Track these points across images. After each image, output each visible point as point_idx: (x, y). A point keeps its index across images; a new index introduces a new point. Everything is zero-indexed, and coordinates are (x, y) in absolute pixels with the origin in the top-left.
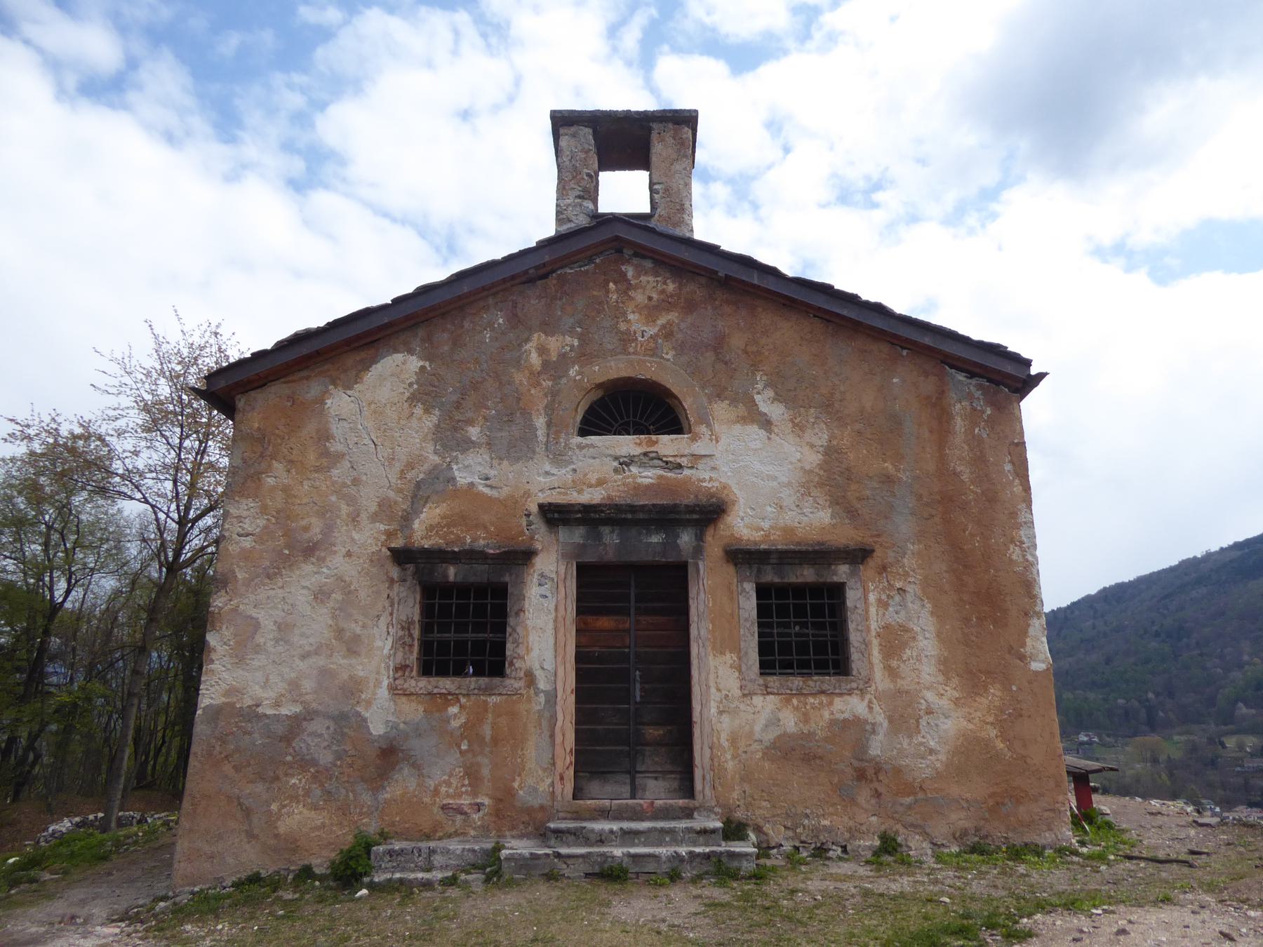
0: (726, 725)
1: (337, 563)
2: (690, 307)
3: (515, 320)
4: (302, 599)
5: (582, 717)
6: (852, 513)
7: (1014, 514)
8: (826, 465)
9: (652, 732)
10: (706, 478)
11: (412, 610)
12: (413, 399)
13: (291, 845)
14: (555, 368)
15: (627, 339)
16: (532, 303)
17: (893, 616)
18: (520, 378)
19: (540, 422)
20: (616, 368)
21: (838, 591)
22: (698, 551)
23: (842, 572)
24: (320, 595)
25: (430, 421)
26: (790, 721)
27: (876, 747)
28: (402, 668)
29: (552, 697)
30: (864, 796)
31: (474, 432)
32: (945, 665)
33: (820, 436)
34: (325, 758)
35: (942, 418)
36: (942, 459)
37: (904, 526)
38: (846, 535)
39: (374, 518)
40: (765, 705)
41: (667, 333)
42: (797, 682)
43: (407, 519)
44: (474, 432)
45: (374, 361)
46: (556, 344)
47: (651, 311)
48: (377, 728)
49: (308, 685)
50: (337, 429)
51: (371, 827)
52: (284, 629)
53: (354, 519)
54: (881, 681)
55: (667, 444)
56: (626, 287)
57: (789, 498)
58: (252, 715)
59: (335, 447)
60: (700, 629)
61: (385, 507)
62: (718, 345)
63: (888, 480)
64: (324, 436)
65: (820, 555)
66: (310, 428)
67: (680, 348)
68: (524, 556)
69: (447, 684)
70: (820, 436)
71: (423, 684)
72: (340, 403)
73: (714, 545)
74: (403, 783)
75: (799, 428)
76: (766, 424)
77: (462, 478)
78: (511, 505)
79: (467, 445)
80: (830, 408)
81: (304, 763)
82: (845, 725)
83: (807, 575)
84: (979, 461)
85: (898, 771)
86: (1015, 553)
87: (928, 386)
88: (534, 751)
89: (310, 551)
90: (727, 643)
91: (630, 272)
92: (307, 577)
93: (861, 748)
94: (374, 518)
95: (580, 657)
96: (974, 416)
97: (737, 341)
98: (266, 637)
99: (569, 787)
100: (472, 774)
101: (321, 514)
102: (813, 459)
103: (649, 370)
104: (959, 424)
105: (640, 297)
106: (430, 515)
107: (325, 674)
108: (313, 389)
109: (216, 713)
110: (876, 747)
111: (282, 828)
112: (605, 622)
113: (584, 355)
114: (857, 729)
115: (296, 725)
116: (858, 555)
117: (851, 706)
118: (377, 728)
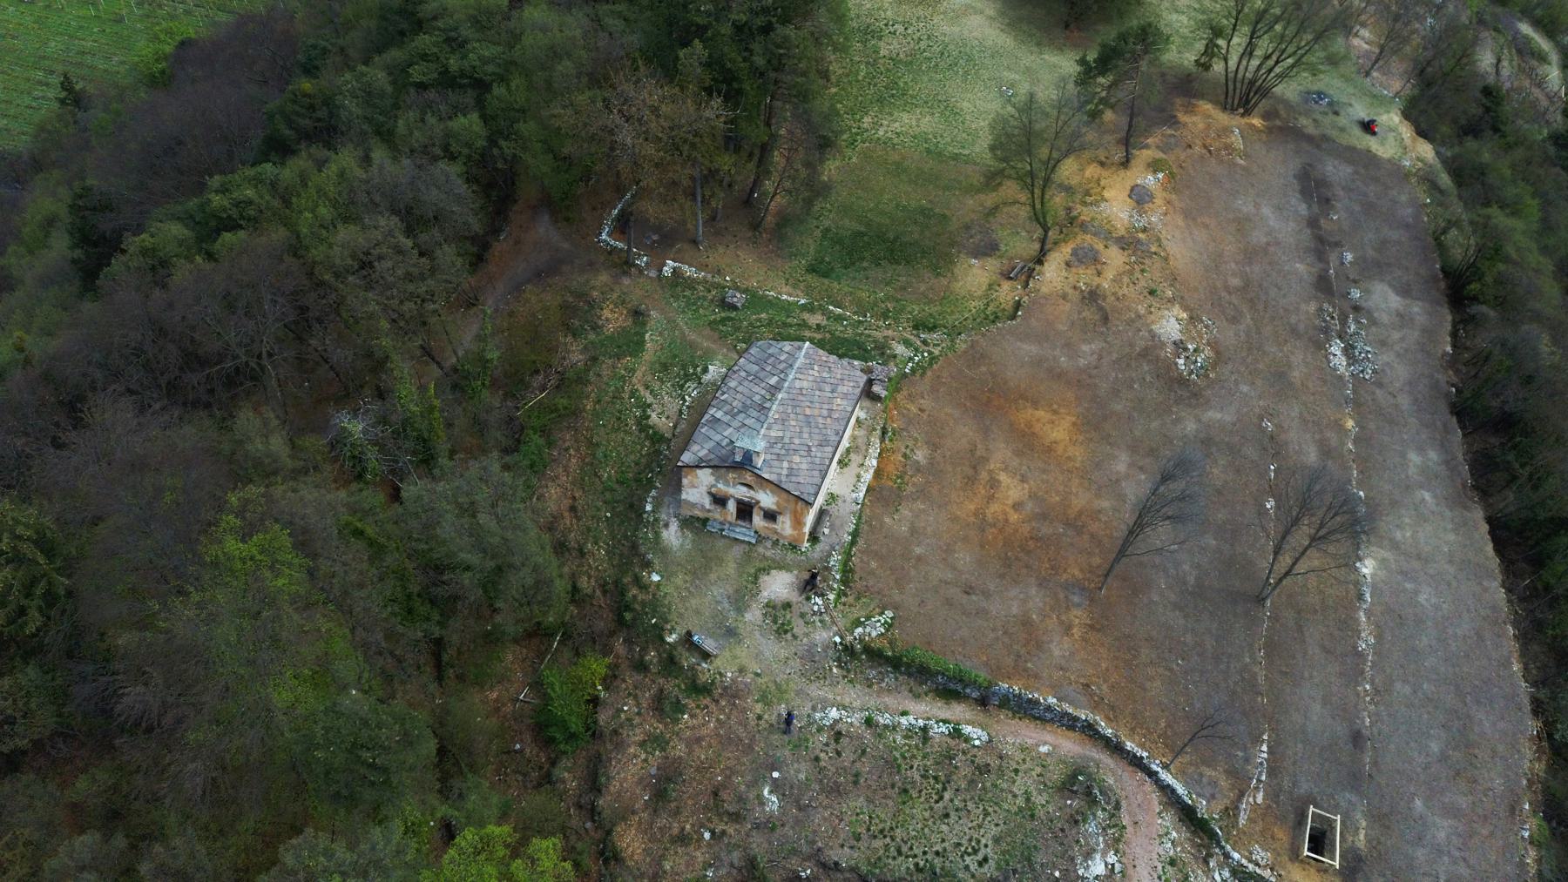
55: (752, 492)
116: (780, 513)
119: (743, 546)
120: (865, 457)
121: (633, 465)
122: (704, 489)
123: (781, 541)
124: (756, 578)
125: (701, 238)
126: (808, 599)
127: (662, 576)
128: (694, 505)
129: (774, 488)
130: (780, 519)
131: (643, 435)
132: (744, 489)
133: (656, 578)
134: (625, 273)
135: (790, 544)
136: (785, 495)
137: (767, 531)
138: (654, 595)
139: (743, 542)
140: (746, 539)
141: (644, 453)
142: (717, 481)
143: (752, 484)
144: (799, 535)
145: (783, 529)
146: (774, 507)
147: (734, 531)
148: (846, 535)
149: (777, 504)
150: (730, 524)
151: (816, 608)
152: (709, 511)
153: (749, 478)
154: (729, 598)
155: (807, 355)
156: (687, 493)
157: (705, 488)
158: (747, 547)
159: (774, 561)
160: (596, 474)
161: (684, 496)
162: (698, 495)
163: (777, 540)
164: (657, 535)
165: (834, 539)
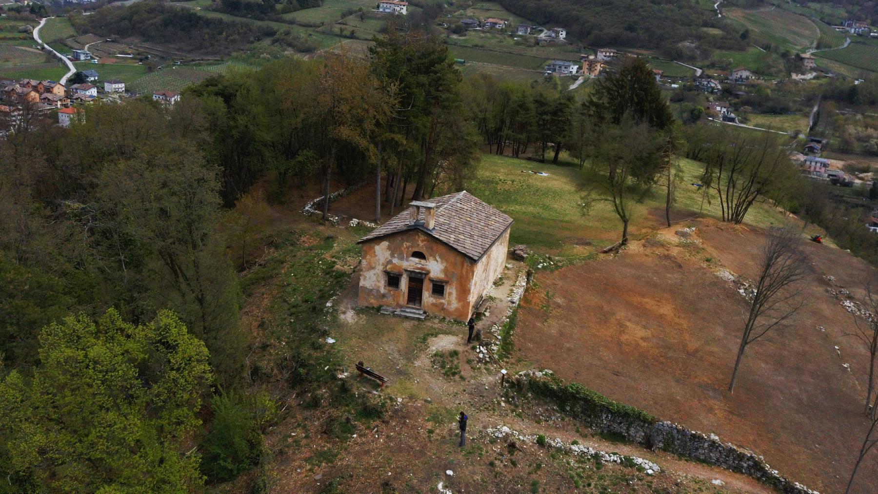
0: (426, 300)
1: (377, 270)
2: (428, 241)
3: (402, 239)
4: (372, 275)
5: (409, 295)
6: (447, 276)
7: (470, 280)
8: (445, 269)
9: (418, 298)
10: (428, 268)
11: (387, 279)
12: (387, 249)
13: (371, 304)
14: (408, 248)
15: (419, 245)
16: (405, 237)
17: (450, 291)
18: (403, 249)
19: (405, 256)
20: (417, 250)
21: (444, 286)
22: (425, 278)
23: (444, 284)
24: (374, 274)
25: (390, 252)
26: (434, 301)
27: (445, 307)
28: (385, 286)
29: (404, 293)
30: (442, 312)
31: (396, 255)
32: (456, 298)
33: (445, 264)
34: (375, 294)
35: (463, 266)
36: (462, 271)
37: (454, 279)
38: (446, 279)
39: (382, 265)
40: (431, 299)
41: (424, 245)
42: (436, 296)
43: (386, 267)
44: (396, 255)
45: (381, 242)
46: (408, 244)
47: (423, 241)
48: (382, 292)
49: (373, 285)
50: (376, 251)
51: (381, 304)
52: (370, 278)
53: (379, 265)
54: (447, 299)
55: (423, 261)
56: (419, 237)
57: (439, 273)
58: (366, 288)
59: (376, 254)
60: (424, 288)
61: (383, 264)
62: (432, 249)
63: (453, 272)
64: (375, 252)
65: (442, 281)
66: (373, 250)
67: (426, 248)
68: (401, 275)
69: (391, 288)
70: (445, 264)
71: (388, 288)
72: (377, 248)
73: (427, 278)
74: (385, 299)
75: (442, 263)
76: (437, 261)
77: (394, 262)
78: (400, 267)
79: (395, 257)
80: (447, 261)
81: (373, 295)
82: (441, 303)
83: (439, 284)
84: (467, 272)
85: (447, 310)
86: (469, 286)
87: (462, 260)
88: (401, 298)
89: (373, 268)
90: (427, 290)
91: (420, 234)
92: (372, 272)
93: (443, 306)
94: (382, 265)
95: (409, 287)
96: (467, 266)
97: (435, 248)
98: (368, 278)
99: (406, 303)
100: (394, 300)
101: (375, 263)
102: (443, 268)
103: (421, 251)
104: (465, 266)
105: (421, 239)
106: (389, 267)
107: (375, 285)
108: (373, 245)
109: (361, 287)
110: (445, 307)
111: (371, 301)
112: (413, 283)
113: (412, 246)
114: (443, 304)
115: (372, 290)
116: (447, 282)
117: (443, 301)
118: (382, 292)
119: (412, 322)
120: (516, 282)
121: (317, 292)
122: (379, 269)
123: (448, 319)
124: (425, 339)
125: (379, 216)
126: (474, 348)
127: (337, 341)
128: (369, 292)
129: (442, 249)
130: (448, 289)
131: (328, 276)
132: (416, 260)
133: (331, 341)
134: (321, 224)
135: (455, 321)
136: (452, 257)
137: (434, 309)
138: (328, 352)
139: (413, 319)
140: (417, 316)
141: (327, 285)
142: (392, 255)
143: (424, 251)
144: (463, 307)
145: (449, 303)
146: (442, 276)
147: (405, 311)
148: (504, 318)
149: (445, 271)
150: (401, 307)
151: (481, 356)
152: (384, 296)
153: (421, 244)
154: (399, 351)
155: (465, 195)
156: (365, 278)
157: (381, 268)
158: (416, 323)
159: (440, 330)
160: (285, 301)
161: (361, 283)
162: (374, 278)
163: (444, 318)
164: (335, 318)
165: (495, 319)
